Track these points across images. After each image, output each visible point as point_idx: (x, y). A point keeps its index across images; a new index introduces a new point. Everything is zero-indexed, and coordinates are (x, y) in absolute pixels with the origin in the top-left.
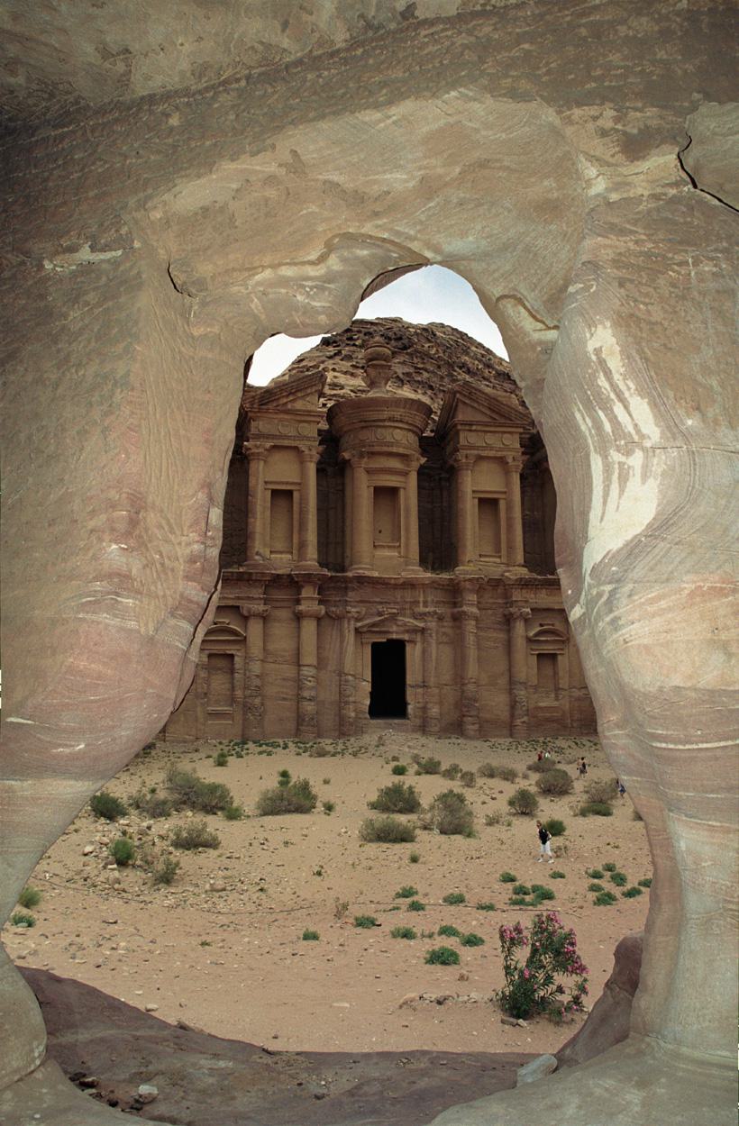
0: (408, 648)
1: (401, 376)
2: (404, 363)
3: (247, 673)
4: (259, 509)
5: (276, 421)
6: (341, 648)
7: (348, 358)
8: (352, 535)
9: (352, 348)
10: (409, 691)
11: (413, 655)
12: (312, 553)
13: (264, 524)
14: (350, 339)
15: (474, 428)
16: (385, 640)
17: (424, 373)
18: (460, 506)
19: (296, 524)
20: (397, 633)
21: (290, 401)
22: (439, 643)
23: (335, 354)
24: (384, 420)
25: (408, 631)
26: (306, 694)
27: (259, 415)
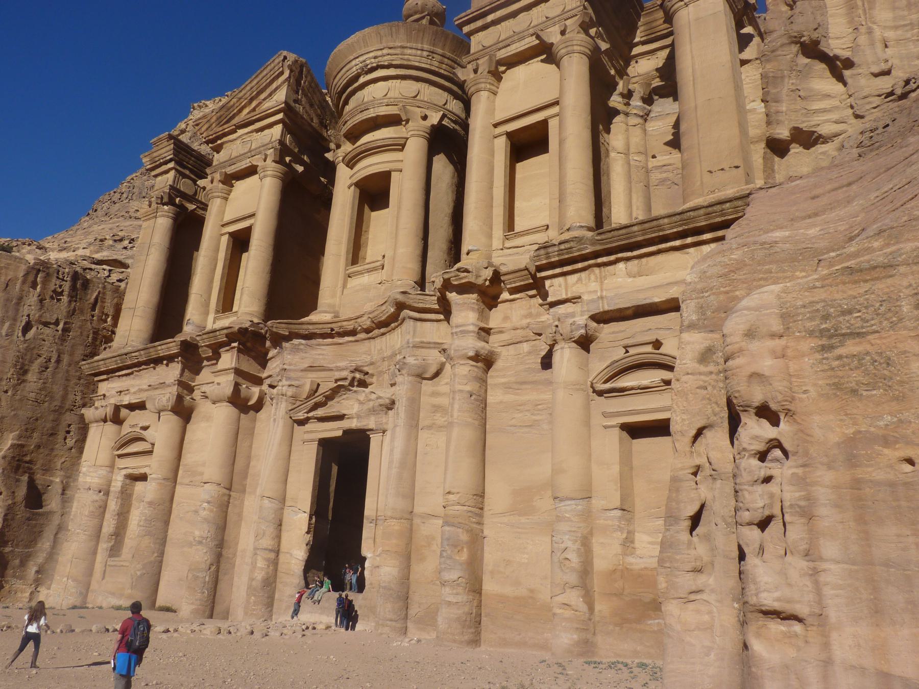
0: (375, 440)
5: (238, 142)
15: (490, 18)
16: (339, 433)
20: (359, 417)
21: (254, 110)
24: (356, 78)
25: (373, 411)
27: (219, 142)
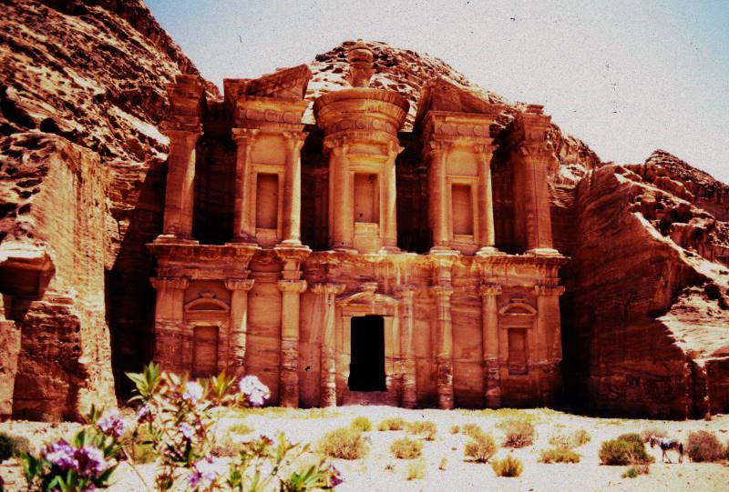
1: (386, 87)
2: (389, 77)
3: (231, 343)
4: (245, 189)
6: (322, 321)
7: (339, 71)
8: (334, 211)
9: (343, 63)
10: (387, 364)
11: (391, 328)
12: (296, 231)
13: (250, 204)
14: (342, 56)
17: (407, 86)
18: (435, 191)
19: (280, 204)
22: (415, 318)
23: (328, 68)
26: (288, 365)
